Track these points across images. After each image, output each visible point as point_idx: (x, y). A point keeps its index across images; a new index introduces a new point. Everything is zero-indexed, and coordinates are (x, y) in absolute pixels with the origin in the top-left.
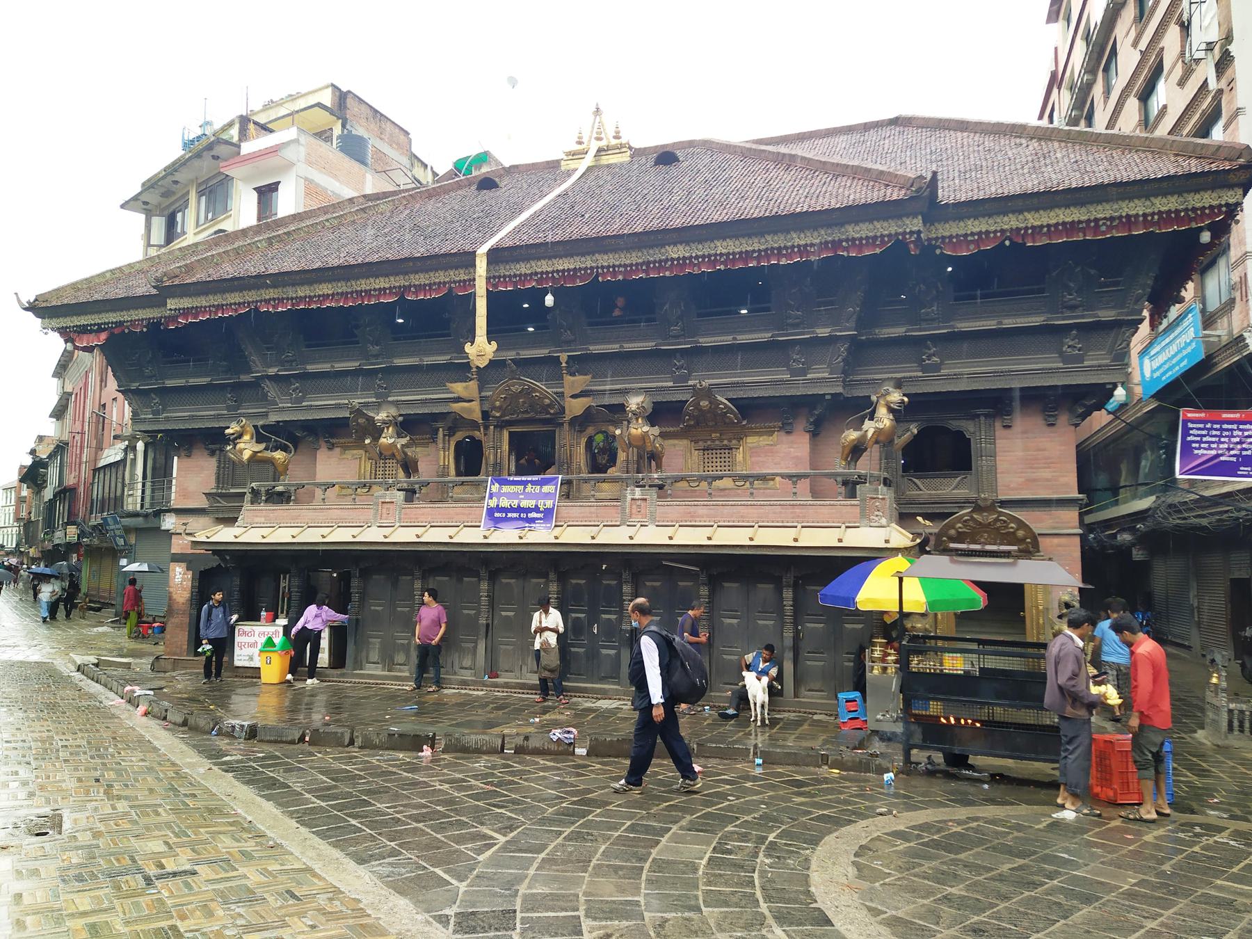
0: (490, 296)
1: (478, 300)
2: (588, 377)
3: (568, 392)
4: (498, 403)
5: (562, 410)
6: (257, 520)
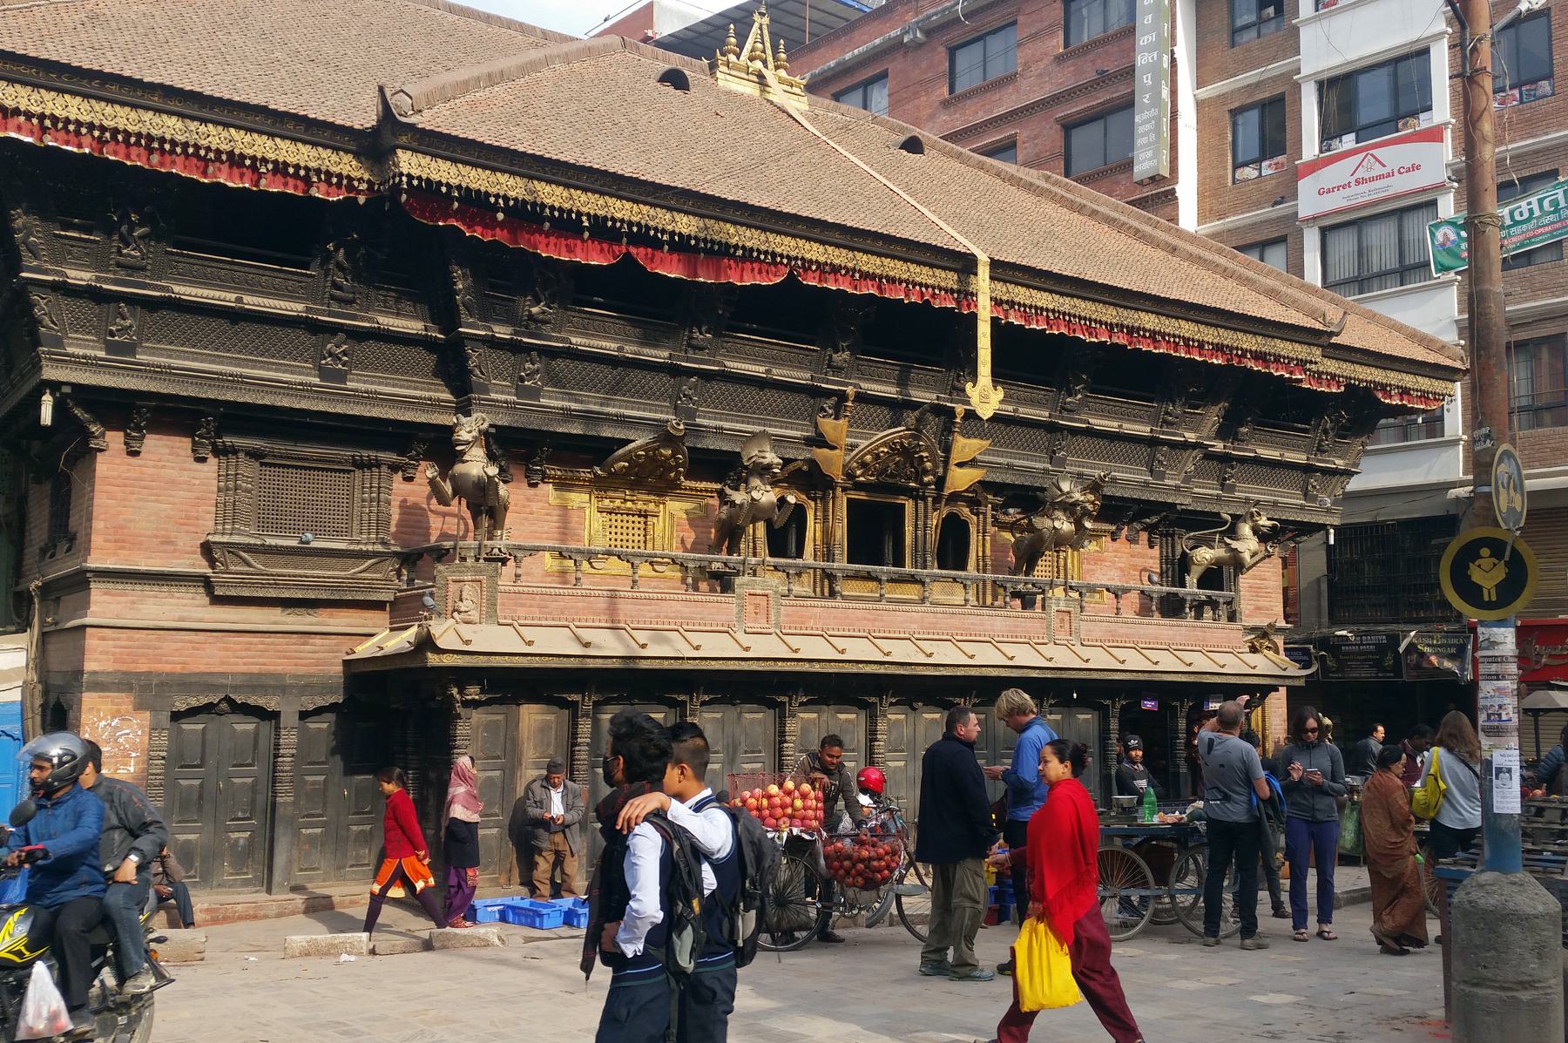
0: (995, 322)
1: (980, 324)
2: (986, 443)
3: (956, 457)
4: (868, 458)
5: (941, 482)
6: (521, 612)
